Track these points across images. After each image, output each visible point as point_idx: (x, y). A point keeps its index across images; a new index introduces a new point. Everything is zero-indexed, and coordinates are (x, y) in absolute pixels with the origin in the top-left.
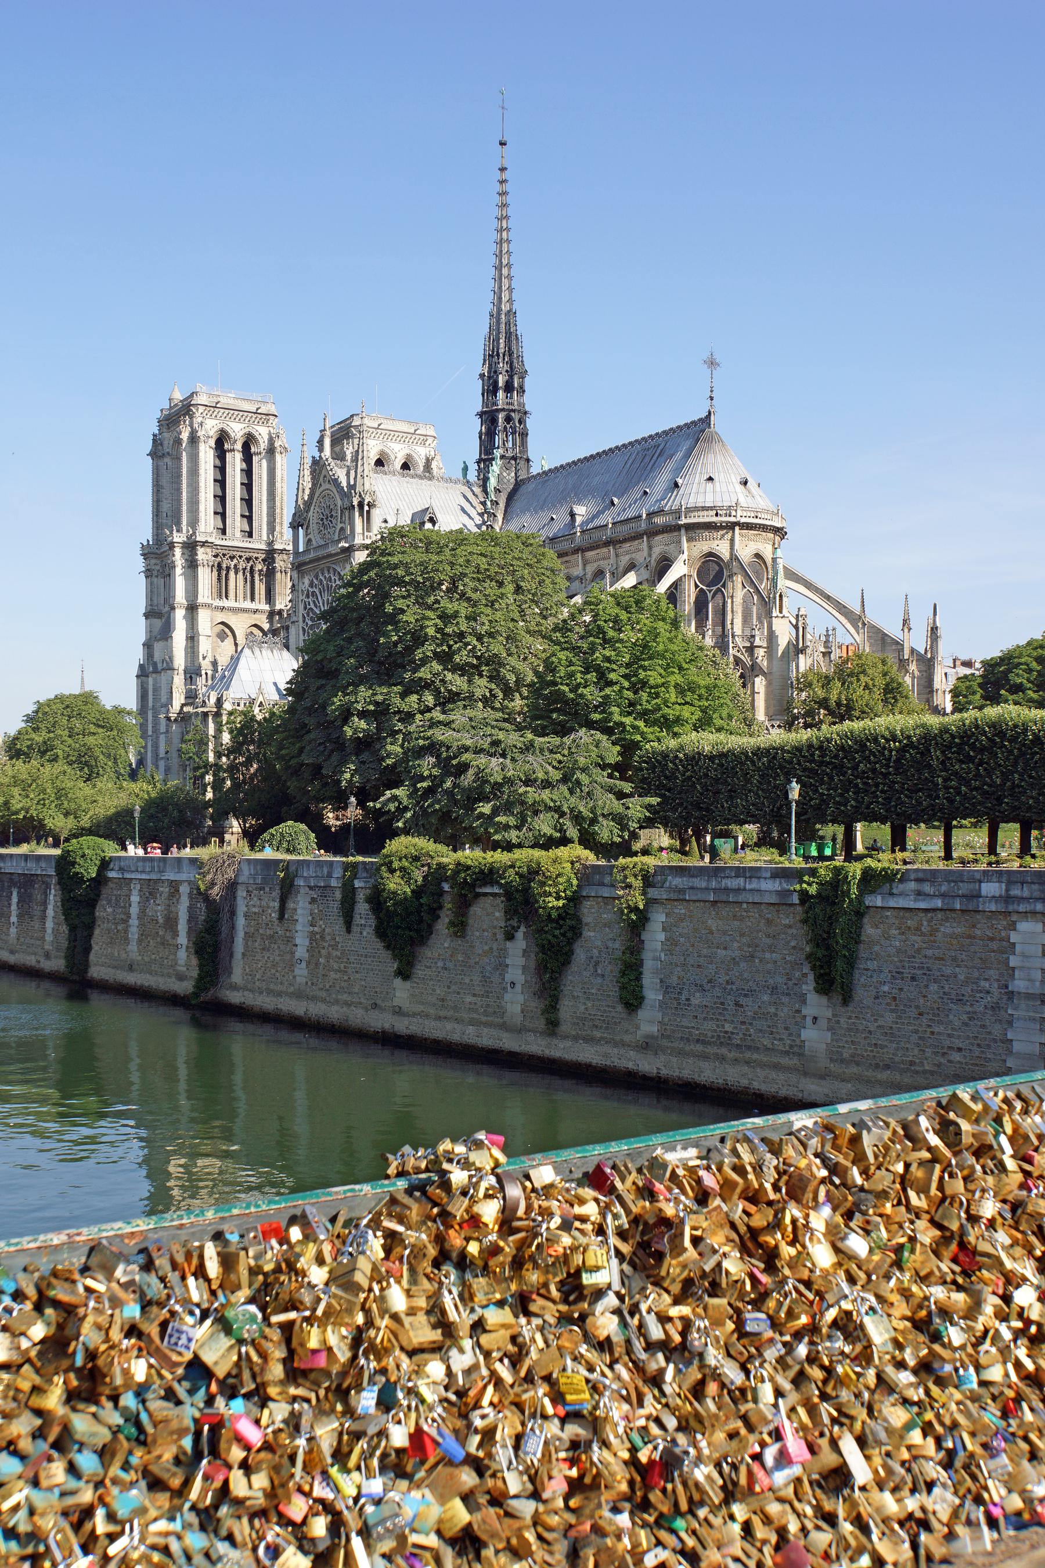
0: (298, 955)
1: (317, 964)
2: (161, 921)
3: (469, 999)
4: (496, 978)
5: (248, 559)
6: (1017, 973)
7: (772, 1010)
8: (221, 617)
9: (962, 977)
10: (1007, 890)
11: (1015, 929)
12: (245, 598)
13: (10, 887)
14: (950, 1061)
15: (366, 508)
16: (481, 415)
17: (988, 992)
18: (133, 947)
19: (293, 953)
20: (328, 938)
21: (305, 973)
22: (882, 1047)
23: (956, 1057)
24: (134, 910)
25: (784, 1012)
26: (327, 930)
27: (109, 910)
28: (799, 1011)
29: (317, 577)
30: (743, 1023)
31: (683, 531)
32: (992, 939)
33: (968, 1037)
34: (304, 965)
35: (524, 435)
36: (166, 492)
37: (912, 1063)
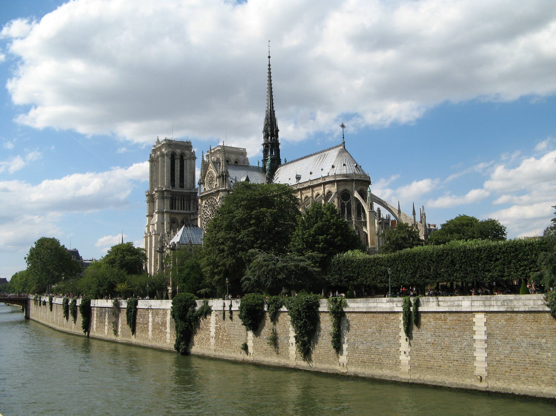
2: (160, 323)
4: (286, 342)
5: (183, 196)
6: (476, 332)
7: (388, 349)
8: (173, 216)
9: (457, 335)
10: (471, 304)
11: (475, 317)
12: (181, 209)
13: (105, 312)
14: (454, 365)
15: (225, 177)
16: (263, 145)
17: (466, 340)
18: (150, 333)
21: (214, 341)
23: (455, 363)
24: (151, 319)
25: (393, 350)
27: (141, 320)
28: (399, 350)
29: (207, 201)
32: (467, 321)
33: (460, 356)
34: (214, 338)
35: (278, 151)
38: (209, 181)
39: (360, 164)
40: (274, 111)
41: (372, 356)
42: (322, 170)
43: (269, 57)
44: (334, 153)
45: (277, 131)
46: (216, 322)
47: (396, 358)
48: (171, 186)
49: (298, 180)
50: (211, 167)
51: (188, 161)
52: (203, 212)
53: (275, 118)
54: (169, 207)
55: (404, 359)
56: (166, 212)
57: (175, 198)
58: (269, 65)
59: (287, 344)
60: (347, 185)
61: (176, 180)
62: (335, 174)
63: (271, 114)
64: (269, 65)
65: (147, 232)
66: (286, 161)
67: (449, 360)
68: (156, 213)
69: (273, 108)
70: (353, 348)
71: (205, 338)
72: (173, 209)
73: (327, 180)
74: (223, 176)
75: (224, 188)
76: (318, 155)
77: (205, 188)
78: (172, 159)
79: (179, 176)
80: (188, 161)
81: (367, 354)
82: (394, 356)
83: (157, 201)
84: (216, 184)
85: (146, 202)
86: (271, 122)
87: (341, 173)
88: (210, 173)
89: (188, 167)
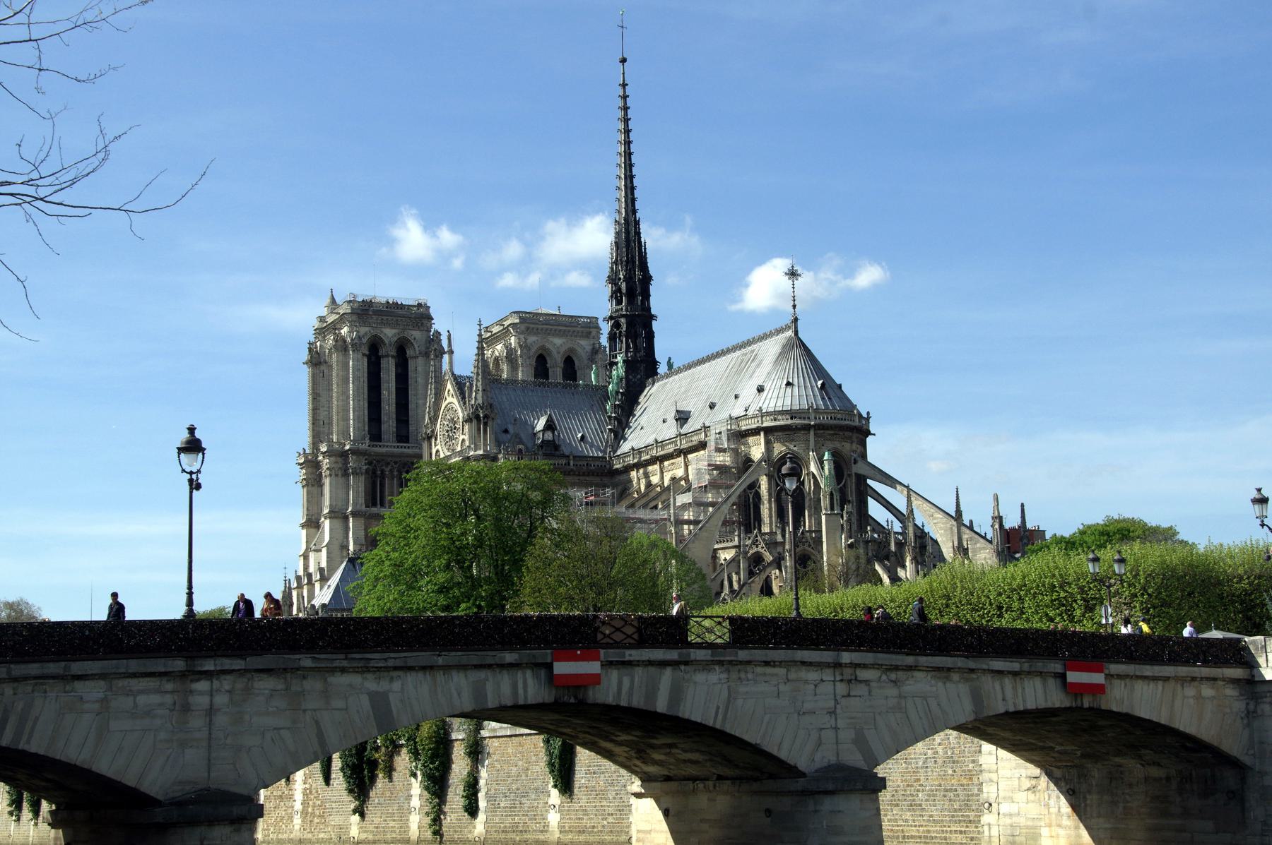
0: (295, 808)
1: (307, 813)
3: (392, 824)
14: (608, 823)
17: (623, 776)
19: (293, 807)
20: (314, 791)
22: (582, 819)
23: (610, 819)
26: (314, 785)
28: (547, 803)
30: (523, 815)
31: (762, 434)
34: (299, 813)
35: (650, 336)
36: (323, 400)
37: (594, 827)
38: (447, 431)
40: (637, 223)
41: (516, 818)
42: (736, 397)
43: (624, 61)
44: (772, 348)
45: (647, 279)
46: (304, 778)
47: (544, 819)
48: (367, 439)
49: (681, 428)
50: (451, 390)
51: (421, 361)
53: (640, 242)
54: (361, 500)
55: (554, 818)
56: (354, 514)
57: (383, 471)
58: (624, 85)
59: (408, 809)
60: (793, 440)
61: (384, 418)
62: (760, 409)
63: (627, 232)
65: (301, 573)
66: (670, 365)
67: (603, 815)
68: (325, 519)
69: (634, 211)
70: (494, 807)
71: (286, 818)
72: (374, 505)
74: (477, 417)
75: (481, 452)
76: (738, 353)
77: (438, 451)
78: (373, 359)
79: (393, 408)
80: (421, 361)
81: (510, 816)
82: (542, 815)
83: (327, 482)
84: (463, 440)
85: (300, 485)
86: (627, 256)
87: (777, 409)
88: (450, 408)
89: (419, 380)
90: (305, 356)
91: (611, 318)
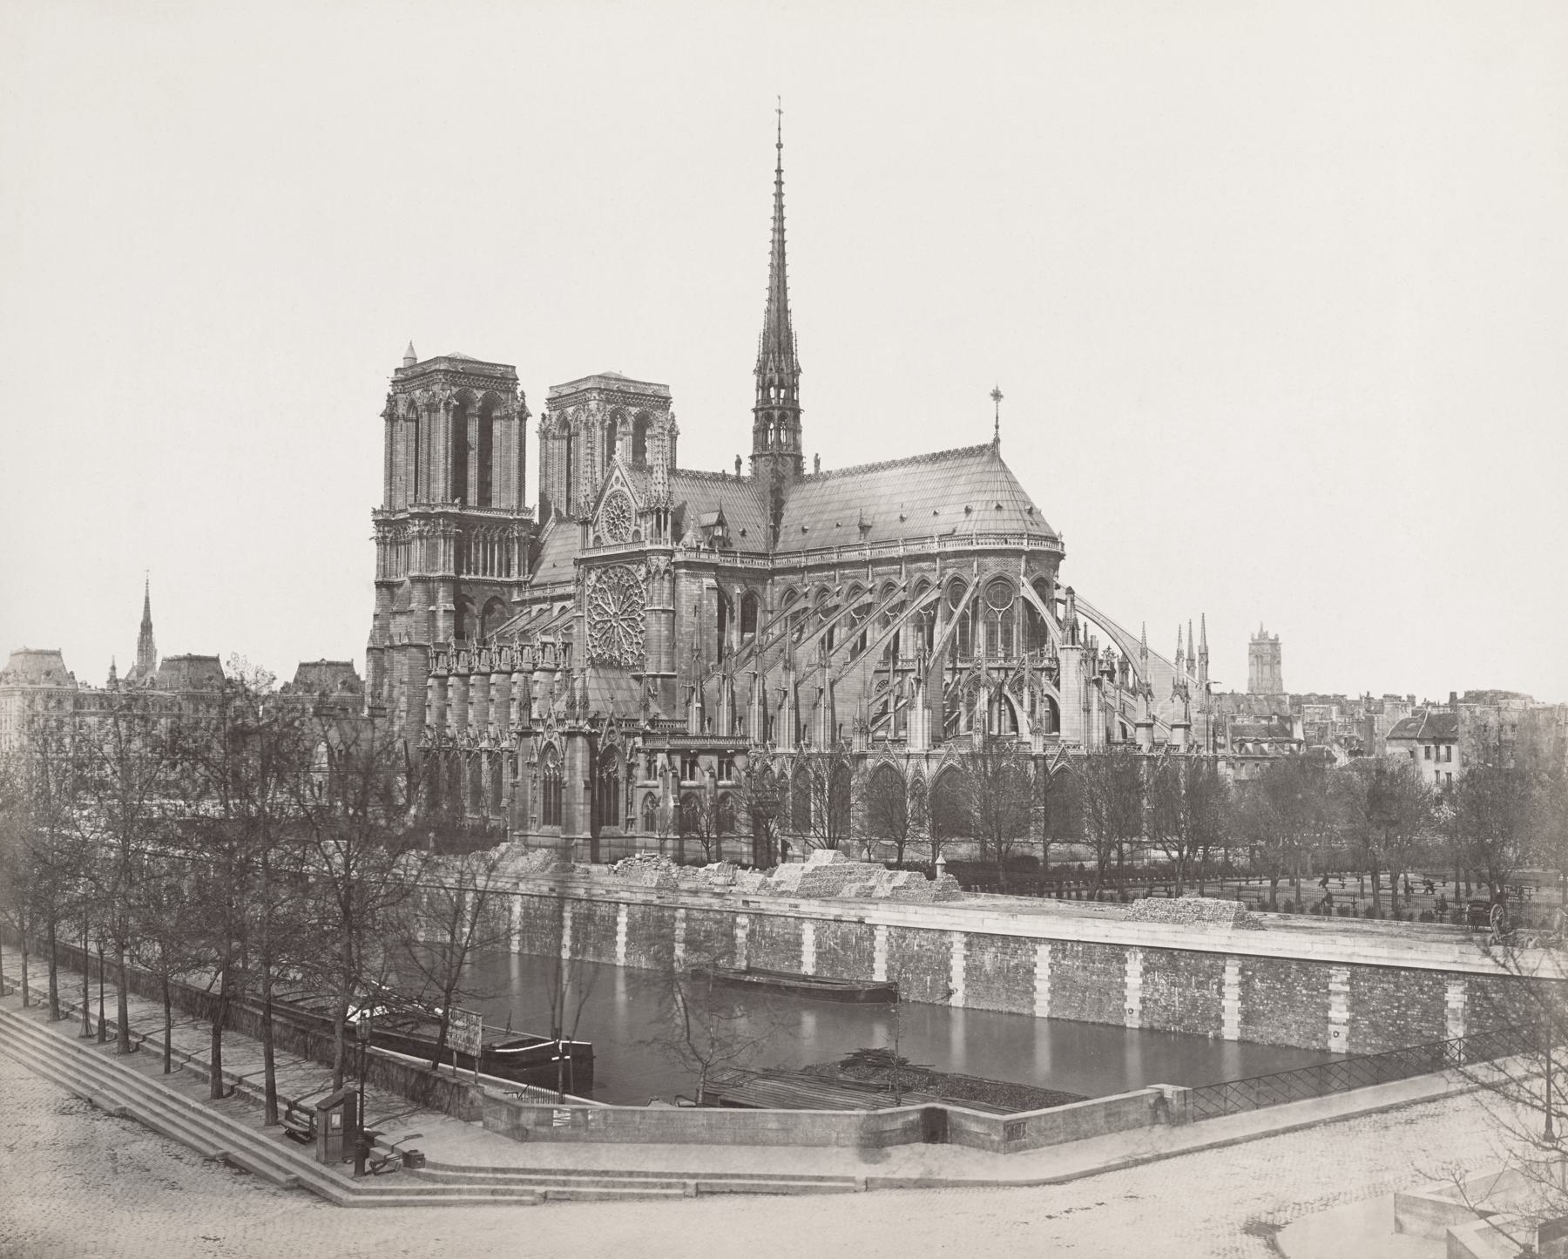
12: (485, 569)
35: (796, 430)
39: (1038, 505)
43: (779, 146)
45: (796, 373)
52: (590, 603)
58: (779, 171)
64: (779, 171)
69: (786, 301)
73: (950, 547)
85: (373, 541)
90: (382, 405)
91: (762, 409)
